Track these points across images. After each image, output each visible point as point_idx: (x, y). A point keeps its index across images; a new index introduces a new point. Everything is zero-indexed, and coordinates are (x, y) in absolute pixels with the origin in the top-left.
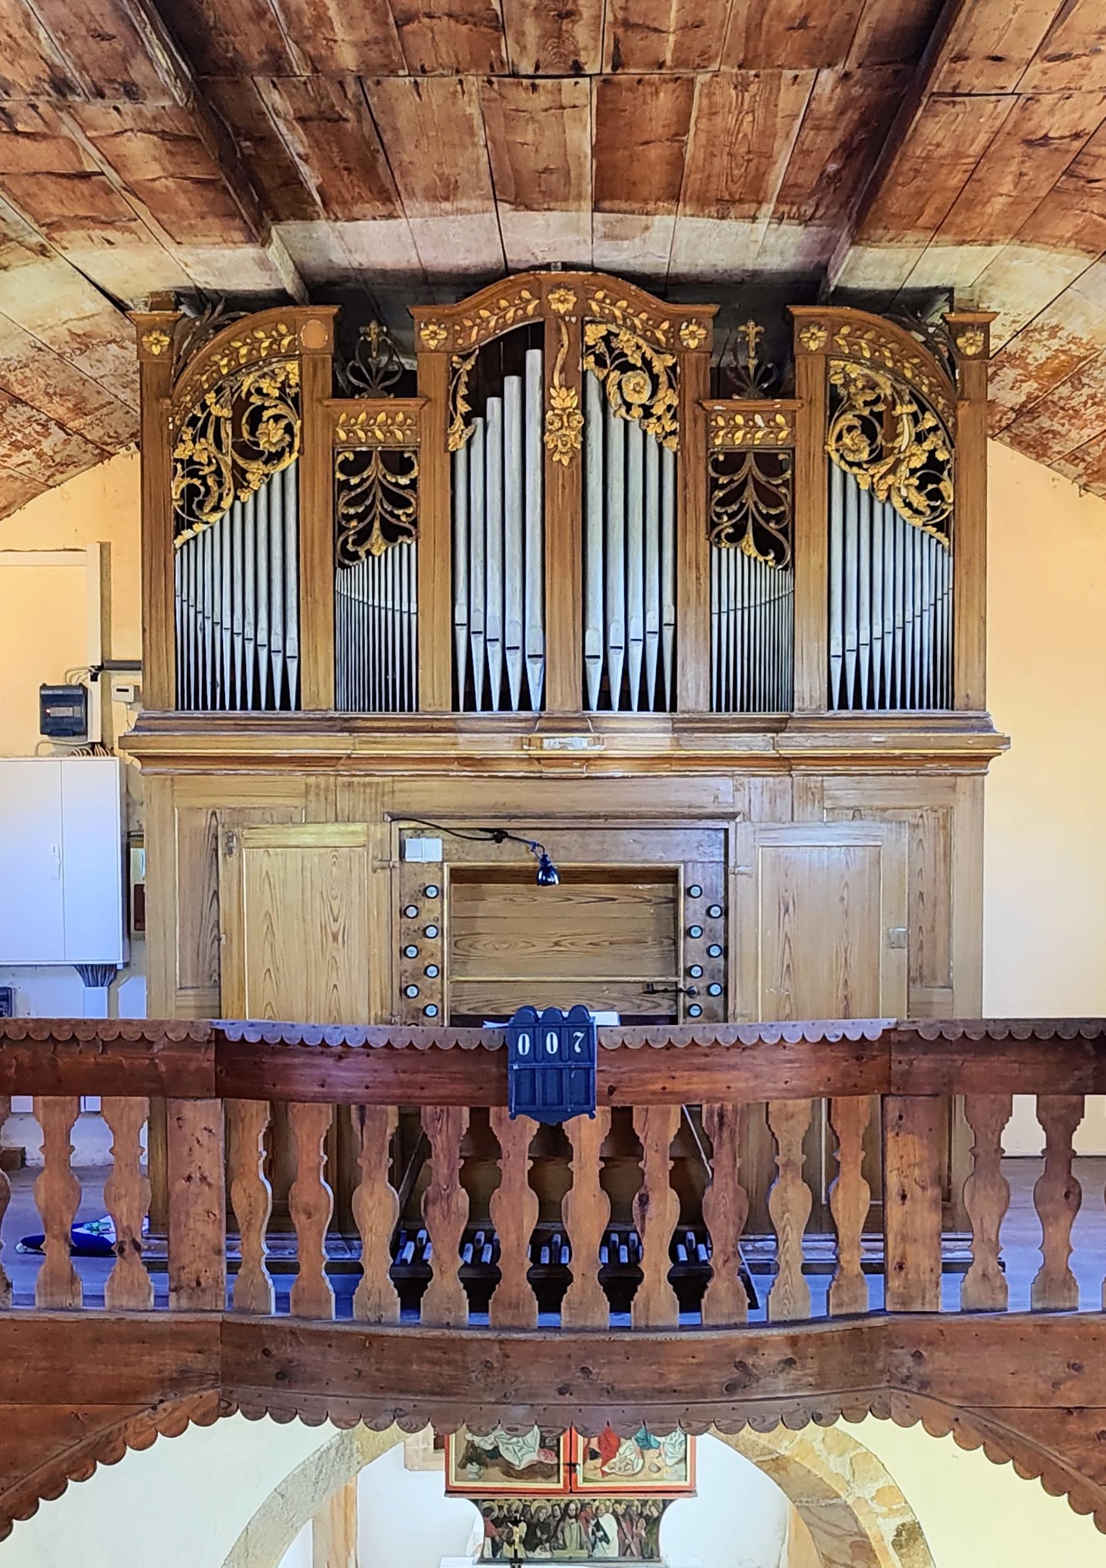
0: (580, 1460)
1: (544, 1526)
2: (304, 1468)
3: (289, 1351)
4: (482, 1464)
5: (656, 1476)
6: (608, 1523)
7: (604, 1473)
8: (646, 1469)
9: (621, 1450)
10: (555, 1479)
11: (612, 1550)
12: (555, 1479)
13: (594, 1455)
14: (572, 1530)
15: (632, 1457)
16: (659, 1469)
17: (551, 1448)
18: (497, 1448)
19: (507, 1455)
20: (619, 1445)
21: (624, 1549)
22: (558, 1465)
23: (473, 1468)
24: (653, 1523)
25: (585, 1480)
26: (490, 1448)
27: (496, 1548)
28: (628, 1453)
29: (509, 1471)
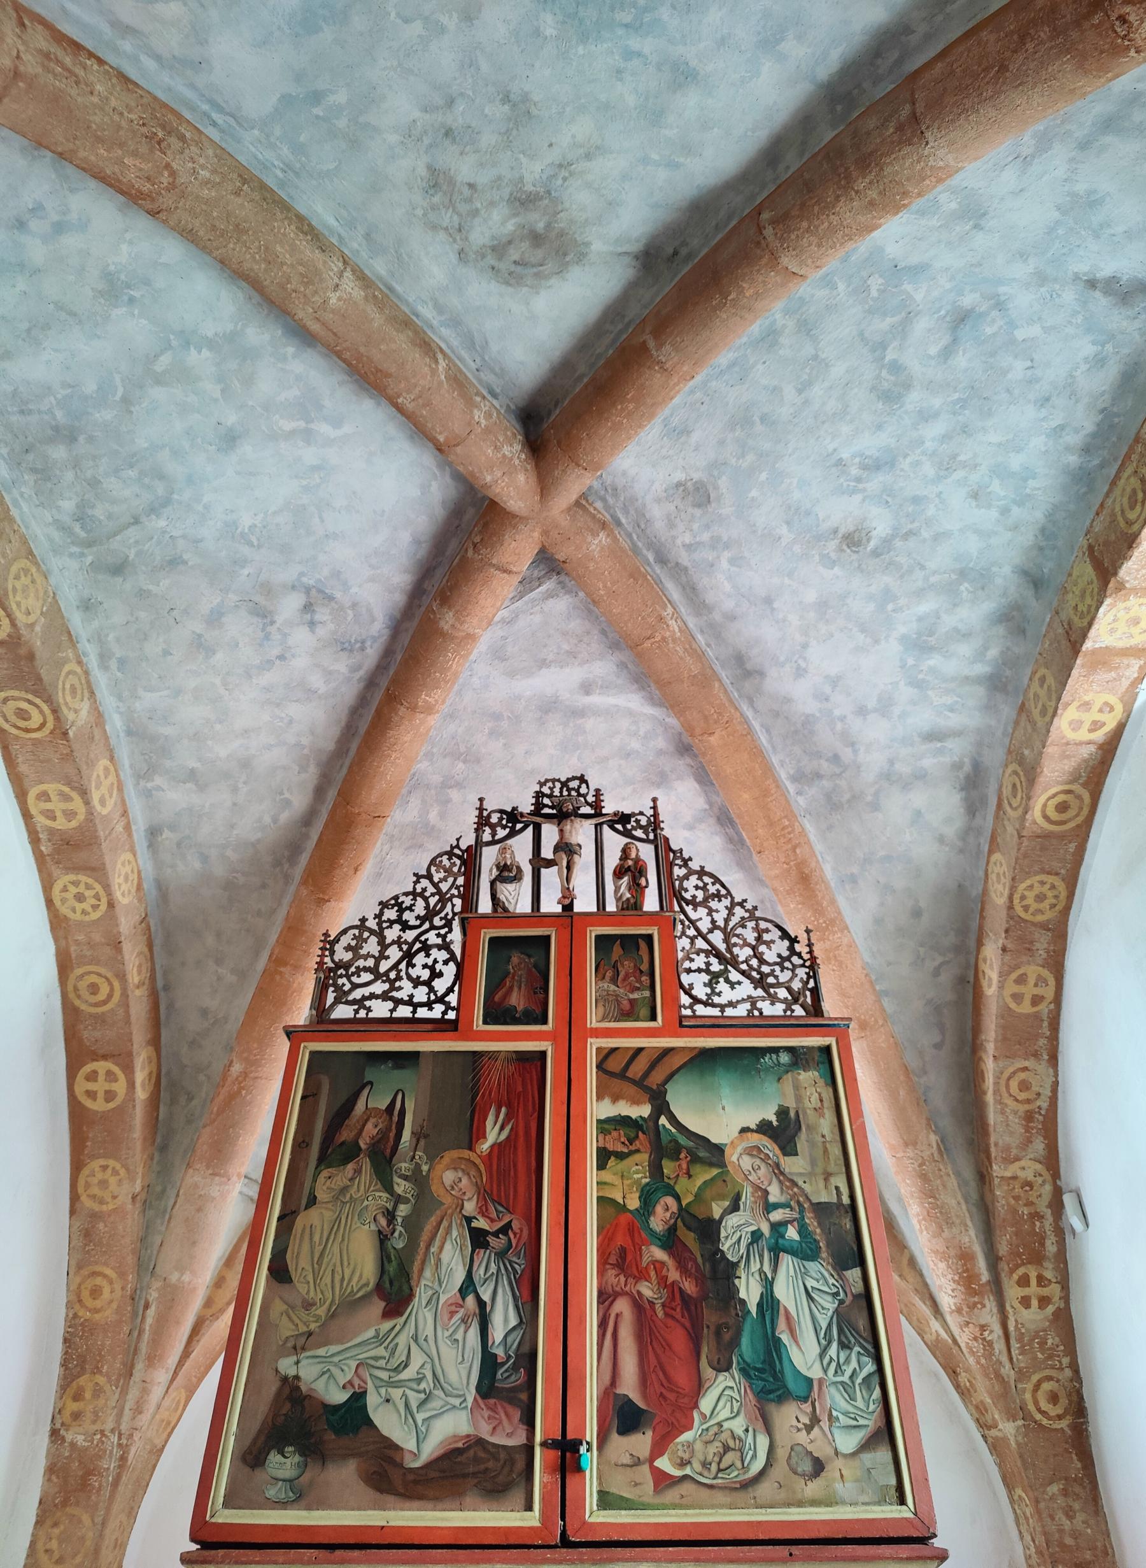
0: (591, 1432)
4: (313, 1451)
5: (813, 1488)
7: (662, 1481)
8: (780, 1470)
9: (706, 1404)
10: (518, 1496)
12: (518, 1496)
13: (624, 1417)
15: (738, 1425)
16: (819, 1467)
17: (508, 1396)
18: (359, 1397)
19: (388, 1421)
20: (698, 1388)
22: (529, 1449)
23: (283, 1465)
25: (606, 1500)
26: (338, 1397)
28: (725, 1413)
29: (388, 1474)
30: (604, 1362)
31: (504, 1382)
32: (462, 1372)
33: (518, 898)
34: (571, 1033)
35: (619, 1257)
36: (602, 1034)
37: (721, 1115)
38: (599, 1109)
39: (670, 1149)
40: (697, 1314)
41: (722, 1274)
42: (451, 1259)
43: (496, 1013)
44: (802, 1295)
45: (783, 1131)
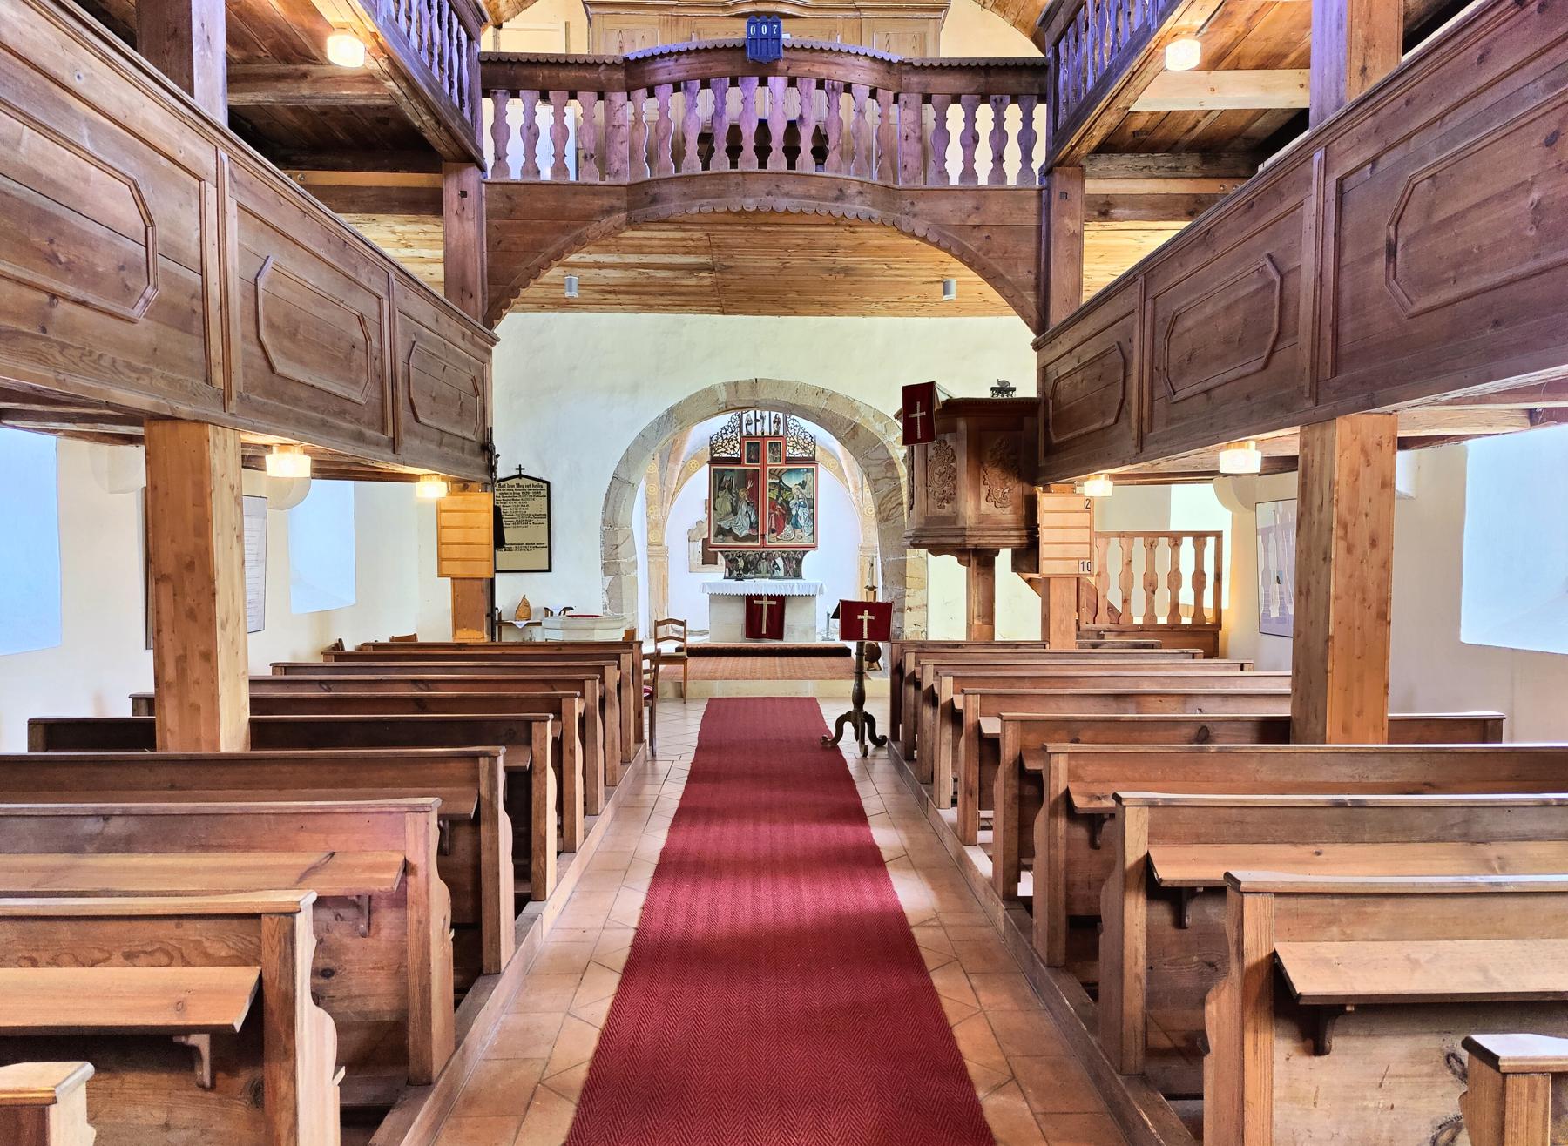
1: (752, 563)
2: (652, 425)
3: (656, 190)
6: (780, 562)
11: (781, 574)
14: (764, 565)
21: (787, 573)
24: (799, 562)
27: (731, 572)
29: (736, 538)
30: (769, 523)
31: (754, 526)
32: (747, 524)
33: (752, 429)
34: (764, 466)
35: (772, 507)
36: (770, 465)
37: (792, 482)
38: (769, 481)
39: (781, 488)
40: (784, 515)
41: (790, 510)
42: (744, 507)
43: (749, 460)
44: (802, 513)
45: (803, 485)
